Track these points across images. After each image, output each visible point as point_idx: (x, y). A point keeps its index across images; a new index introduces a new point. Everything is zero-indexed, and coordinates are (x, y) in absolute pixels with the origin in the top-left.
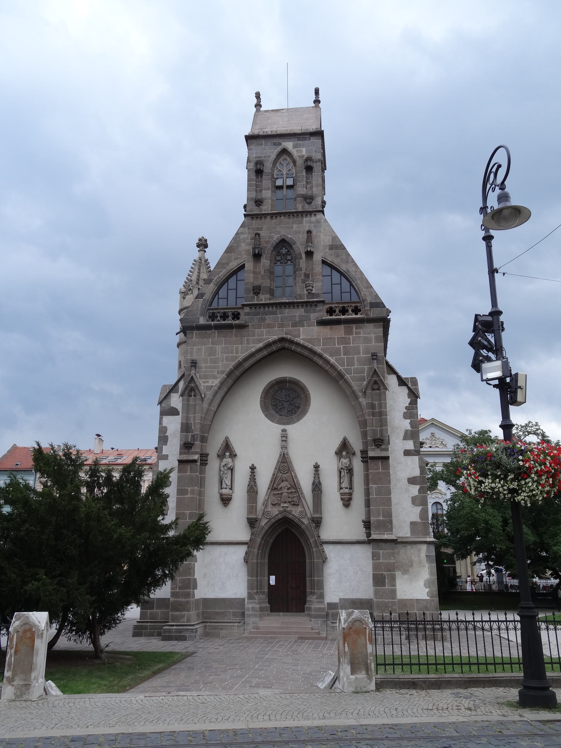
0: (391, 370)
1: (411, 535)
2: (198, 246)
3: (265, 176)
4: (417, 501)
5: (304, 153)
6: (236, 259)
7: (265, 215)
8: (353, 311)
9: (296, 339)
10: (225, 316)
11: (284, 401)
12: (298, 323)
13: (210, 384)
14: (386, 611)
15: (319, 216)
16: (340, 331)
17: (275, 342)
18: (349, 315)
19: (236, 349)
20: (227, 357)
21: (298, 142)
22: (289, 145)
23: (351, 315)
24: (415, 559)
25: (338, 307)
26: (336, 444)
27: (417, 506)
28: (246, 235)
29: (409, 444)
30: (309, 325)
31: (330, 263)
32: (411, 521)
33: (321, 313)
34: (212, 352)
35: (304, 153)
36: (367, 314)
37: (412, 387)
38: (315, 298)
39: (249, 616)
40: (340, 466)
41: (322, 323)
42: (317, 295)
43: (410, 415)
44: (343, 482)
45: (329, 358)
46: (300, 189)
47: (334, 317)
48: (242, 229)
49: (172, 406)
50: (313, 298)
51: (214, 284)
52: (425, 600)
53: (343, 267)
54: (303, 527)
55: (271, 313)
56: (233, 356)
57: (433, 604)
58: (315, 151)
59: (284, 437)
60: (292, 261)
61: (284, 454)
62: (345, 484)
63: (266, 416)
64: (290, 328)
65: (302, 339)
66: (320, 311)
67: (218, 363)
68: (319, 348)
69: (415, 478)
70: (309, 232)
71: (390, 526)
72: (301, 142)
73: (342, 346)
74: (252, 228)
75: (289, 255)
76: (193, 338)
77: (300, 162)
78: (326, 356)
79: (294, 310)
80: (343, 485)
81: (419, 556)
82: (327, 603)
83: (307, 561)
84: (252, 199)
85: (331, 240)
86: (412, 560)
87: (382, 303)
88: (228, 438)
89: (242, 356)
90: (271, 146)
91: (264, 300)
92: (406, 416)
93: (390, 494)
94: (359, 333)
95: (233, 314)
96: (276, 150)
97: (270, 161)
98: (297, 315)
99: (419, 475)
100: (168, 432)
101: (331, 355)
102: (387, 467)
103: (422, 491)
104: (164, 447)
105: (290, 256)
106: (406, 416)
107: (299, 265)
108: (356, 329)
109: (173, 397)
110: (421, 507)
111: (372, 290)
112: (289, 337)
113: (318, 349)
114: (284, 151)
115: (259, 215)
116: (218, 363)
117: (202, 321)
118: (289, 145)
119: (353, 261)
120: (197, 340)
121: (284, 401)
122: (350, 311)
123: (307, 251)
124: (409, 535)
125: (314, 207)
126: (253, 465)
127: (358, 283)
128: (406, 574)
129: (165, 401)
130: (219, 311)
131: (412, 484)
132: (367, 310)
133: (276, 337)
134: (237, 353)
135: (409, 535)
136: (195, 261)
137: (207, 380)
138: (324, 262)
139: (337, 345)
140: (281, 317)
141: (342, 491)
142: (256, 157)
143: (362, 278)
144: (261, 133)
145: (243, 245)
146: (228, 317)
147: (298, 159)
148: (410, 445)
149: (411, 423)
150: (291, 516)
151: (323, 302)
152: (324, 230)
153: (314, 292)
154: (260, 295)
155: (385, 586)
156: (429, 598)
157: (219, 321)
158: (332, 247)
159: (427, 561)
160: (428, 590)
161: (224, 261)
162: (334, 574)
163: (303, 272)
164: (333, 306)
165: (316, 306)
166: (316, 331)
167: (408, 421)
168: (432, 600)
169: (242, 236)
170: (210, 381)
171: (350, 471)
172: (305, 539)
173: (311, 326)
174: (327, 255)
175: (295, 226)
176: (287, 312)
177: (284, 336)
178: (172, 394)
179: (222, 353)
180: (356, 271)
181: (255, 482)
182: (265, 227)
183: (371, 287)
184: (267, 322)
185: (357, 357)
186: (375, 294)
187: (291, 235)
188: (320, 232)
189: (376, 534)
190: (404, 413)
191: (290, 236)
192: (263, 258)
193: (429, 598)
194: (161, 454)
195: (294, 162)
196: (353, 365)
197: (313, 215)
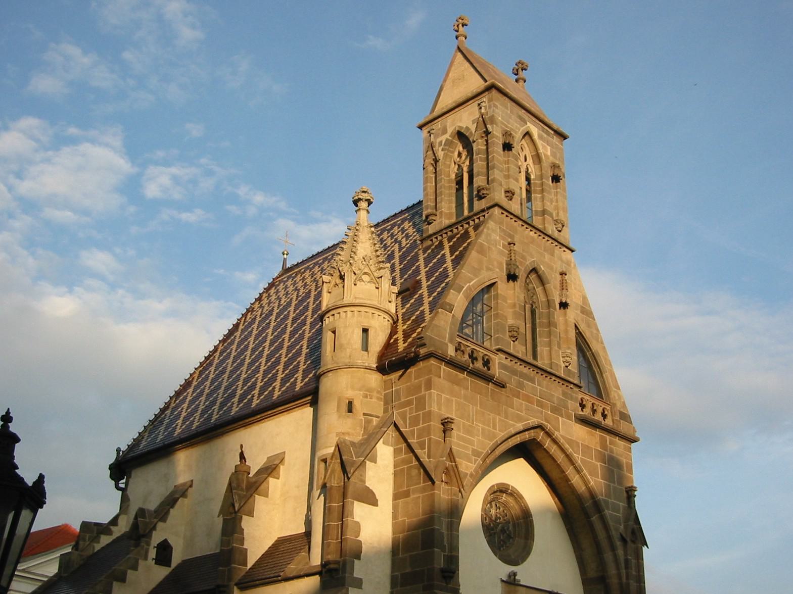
6: (488, 269)
22: (535, 131)
30: (569, 418)
49: (367, 484)
68: (578, 457)
87: (629, 416)
89: (501, 435)
96: (522, 129)
101: (590, 475)
111: (620, 392)
114: (528, 134)
130: (468, 344)
134: (494, 428)
146: (476, 359)
177: (544, 423)
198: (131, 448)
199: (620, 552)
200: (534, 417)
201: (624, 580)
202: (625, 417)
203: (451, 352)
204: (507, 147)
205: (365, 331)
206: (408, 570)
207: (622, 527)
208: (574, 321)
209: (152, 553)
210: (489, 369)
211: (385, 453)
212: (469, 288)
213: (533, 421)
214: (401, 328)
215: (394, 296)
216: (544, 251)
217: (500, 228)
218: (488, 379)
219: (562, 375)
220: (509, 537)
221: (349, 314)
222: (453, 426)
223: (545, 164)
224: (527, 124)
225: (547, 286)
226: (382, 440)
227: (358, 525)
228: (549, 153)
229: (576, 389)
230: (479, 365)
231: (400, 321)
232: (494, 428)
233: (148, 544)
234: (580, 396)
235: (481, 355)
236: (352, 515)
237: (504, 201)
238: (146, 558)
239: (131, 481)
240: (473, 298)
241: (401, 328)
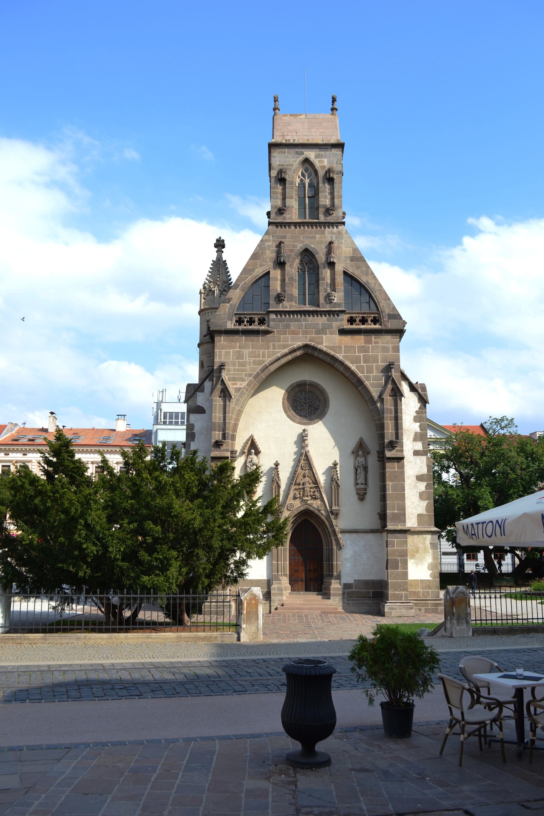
0: (404, 377)
1: (419, 524)
2: (216, 246)
3: (288, 184)
4: (424, 496)
5: (326, 164)
6: (261, 266)
7: (289, 224)
8: (372, 321)
9: (319, 346)
10: (251, 322)
11: (303, 402)
12: (321, 331)
13: (238, 386)
14: (399, 590)
15: (341, 227)
16: (360, 339)
17: (299, 348)
18: (368, 325)
19: (263, 353)
20: (254, 361)
21: (320, 152)
22: (311, 154)
23: (370, 325)
24: (421, 546)
25: (358, 317)
26: (352, 444)
27: (424, 500)
28: (271, 243)
29: (418, 445)
30: (332, 333)
31: (351, 274)
32: (418, 513)
33: (343, 322)
34: (240, 356)
35: (326, 164)
36: (385, 326)
37: (422, 393)
38: (336, 307)
39: (275, 594)
40: (357, 464)
41: (343, 332)
42: (339, 305)
43: (420, 419)
44: (359, 478)
45: (350, 365)
46: (323, 200)
47: (354, 327)
48: (266, 237)
49: (198, 404)
50: (335, 307)
51: (241, 290)
52: (428, 580)
53: (363, 279)
54: (323, 518)
55: (296, 320)
56: (260, 360)
57: (434, 584)
58: (337, 163)
60: (314, 269)
61: (306, 453)
62: (361, 480)
63: (288, 416)
64: (314, 335)
65: (325, 347)
66: (342, 320)
67: (246, 367)
68: (341, 356)
69: (422, 475)
70: (331, 243)
71: (403, 518)
72: (323, 153)
73: (362, 354)
74: (277, 236)
75: (312, 263)
76: (221, 341)
77: (321, 173)
80: (359, 481)
81: (424, 544)
82: (344, 584)
83: (324, 547)
84: (276, 207)
85: (352, 252)
86: (418, 547)
87: (399, 315)
88: (253, 436)
89: (268, 360)
90: (293, 155)
91: (288, 307)
92: (416, 420)
93: (404, 491)
94: (378, 343)
95: (259, 319)
96: (299, 159)
97: (293, 169)
98: (320, 323)
99: (426, 472)
101: (352, 363)
102: (403, 467)
103: (428, 487)
105: (313, 265)
106: (416, 420)
107: (322, 275)
109: (199, 396)
110: (428, 501)
112: (312, 344)
114: (307, 161)
115: (283, 223)
116: (246, 367)
117: (231, 325)
118: (311, 154)
119: (372, 273)
120: (225, 343)
121: (303, 402)
122: (369, 321)
123: (330, 261)
124: (416, 525)
125: (336, 219)
126: (277, 462)
127: (376, 295)
128: (413, 558)
129: (192, 399)
131: (420, 481)
132: (386, 321)
133: (300, 344)
134: (264, 356)
135: (416, 525)
136: (213, 261)
137: (236, 382)
138: (345, 273)
139: (358, 353)
140: (305, 324)
141: (358, 486)
142: (279, 165)
143: (381, 290)
144: (284, 141)
146: (254, 322)
148: (419, 446)
149: (420, 426)
150: (311, 509)
151: (343, 312)
152: (346, 241)
153: (335, 301)
154: (284, 302)
155: (398, 569)
156: (431, 579)
157: (245, 325)
158: (352, 259)
159: (431, 547)
160: (431, 572)
161: (250, 268)
162: (350, 559)
163: (325, 281)
164: (354, 315)
165: (338, 315)
166: (337, 337)
167: (418, 424)
168: (434, 581)
169: (267, 244)
170: (238, 383)
171: (366, 469)
172: (324, 528)
173: (333, 334)
174: (348, 266)
175: (318, 236)
176: (311, 319)
177: (308, 343)
178: (198, 393)
179: (249, 357)
180: (375, 284)
181: (279, 477)
182: (288, 235)
183: (389, 299)
184: (292, 328)
185: (376, 365)
186: (392, 306)
187: (313, 244)
188: (342, 243)
189: (391, 525)
190: (415, 417)
191: (313, 246)
192: (287, 266)
193: (431, 579)
194: (189, 450)
195: (316, 172)
196: (372, 372)
197: (335, 227)
200: (298, 342)
202: (397, 316)
212: (245, 283)
216: (315, 234)
217: (273, 236)
223: (321, 173)
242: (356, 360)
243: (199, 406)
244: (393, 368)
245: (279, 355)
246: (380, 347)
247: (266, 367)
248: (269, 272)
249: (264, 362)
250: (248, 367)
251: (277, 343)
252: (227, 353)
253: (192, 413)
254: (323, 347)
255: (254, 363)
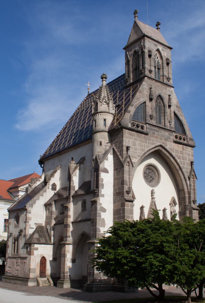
6: (143, 97)
26: (169, 200)
30: (170, 142)
41: (175, 142)
49: (105, 167)
50: (171, 129)
55: (157, 131)
56: (143, 149)
59: (152, 193)
65: (169, 148)
67: (137, 151)
78: (176, 158)
79: (165, 132)
89: (147, 149)
100: (104, 182)
101: (178, 159)
104: (102, 190)
108: (186, 148)
112: (164, 145)
113: (174, 154)
114: (158, 50)
116: (137, 151)
134: (144, 147)
145: (145, 91)
146: (139, 127)
147: (163, 57)
153: (171, 126)
175: (164, 90)
184: (156, 135)
191: (162, 94)
196: (185, 165)
198: (44, 155)
199: (188, 182)
201: (189, 190)
203: (130, 126)
204: (150, 56)
205: (105, 120)
206: (118, 191)
207: (189, 174)
208: (173, 111)
209: (51, 187)
210: (143, 129)
211: (110, 157)
212: (136, 105)
213: (158, 144)
214: (116, 118)
215: (114, 108)
218: (142, 133)
219: (169, 129)
220: (153, 179)
221: (100, 115)
222: (130, 149)
223: (164, 59)
224: (157, 46)
225: (164, 100)
226: (109, 153)
227: (102, 179)
228: (166, 55)
229: (174, 133)
230: (139, 129)
231: (116, 116)
232: (144, 147)
233: (49, 185)
234: (175, 134)
235: (140, 125)
236: (101, 177)
237: (149, 75)
238: (49, 189)
239: (45, 165)
240: (138, 107)
241: (116, 118)
242: (179, 158)
243: (105, 168)
244: (193, 164)
245: (151, 148)
246: (187, 153)
247: (146, 153)
248: (146, 101)
249: (144, 150)
250: (138, 151)
251: (150, 141)
252: (129, 141)
253: (102, 172)
254: (167, 147)
255: (141, 150)
